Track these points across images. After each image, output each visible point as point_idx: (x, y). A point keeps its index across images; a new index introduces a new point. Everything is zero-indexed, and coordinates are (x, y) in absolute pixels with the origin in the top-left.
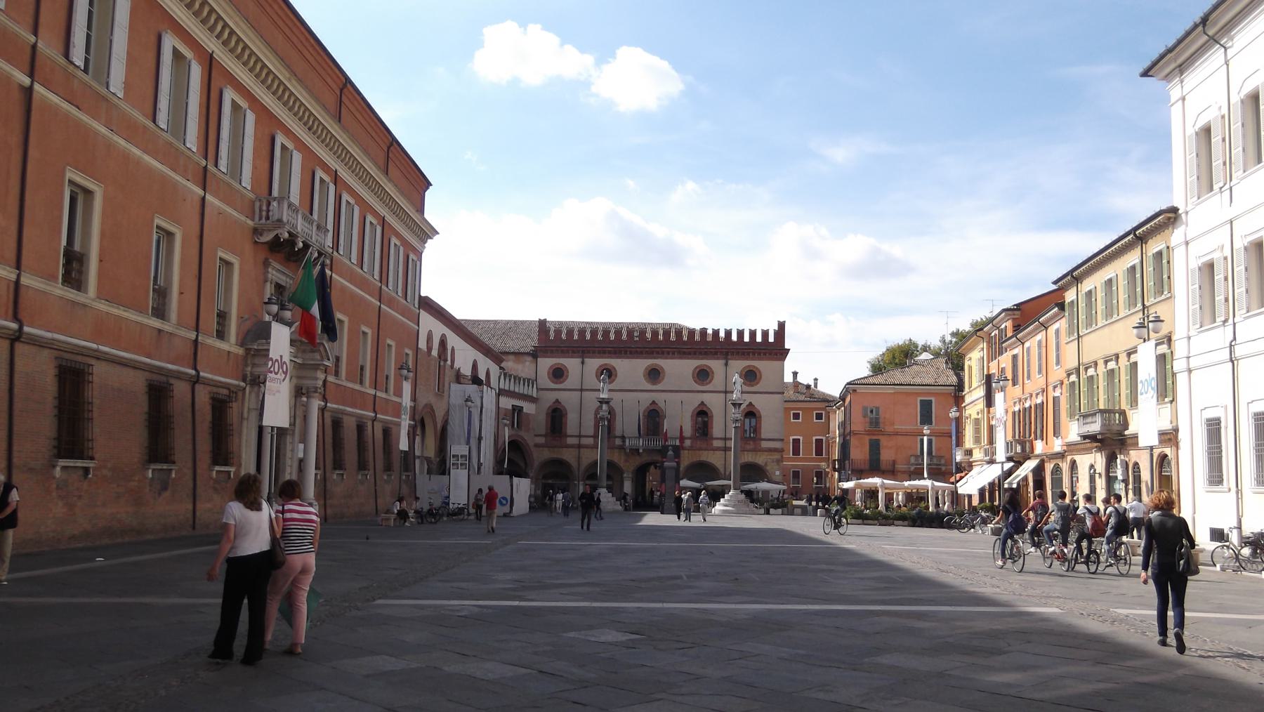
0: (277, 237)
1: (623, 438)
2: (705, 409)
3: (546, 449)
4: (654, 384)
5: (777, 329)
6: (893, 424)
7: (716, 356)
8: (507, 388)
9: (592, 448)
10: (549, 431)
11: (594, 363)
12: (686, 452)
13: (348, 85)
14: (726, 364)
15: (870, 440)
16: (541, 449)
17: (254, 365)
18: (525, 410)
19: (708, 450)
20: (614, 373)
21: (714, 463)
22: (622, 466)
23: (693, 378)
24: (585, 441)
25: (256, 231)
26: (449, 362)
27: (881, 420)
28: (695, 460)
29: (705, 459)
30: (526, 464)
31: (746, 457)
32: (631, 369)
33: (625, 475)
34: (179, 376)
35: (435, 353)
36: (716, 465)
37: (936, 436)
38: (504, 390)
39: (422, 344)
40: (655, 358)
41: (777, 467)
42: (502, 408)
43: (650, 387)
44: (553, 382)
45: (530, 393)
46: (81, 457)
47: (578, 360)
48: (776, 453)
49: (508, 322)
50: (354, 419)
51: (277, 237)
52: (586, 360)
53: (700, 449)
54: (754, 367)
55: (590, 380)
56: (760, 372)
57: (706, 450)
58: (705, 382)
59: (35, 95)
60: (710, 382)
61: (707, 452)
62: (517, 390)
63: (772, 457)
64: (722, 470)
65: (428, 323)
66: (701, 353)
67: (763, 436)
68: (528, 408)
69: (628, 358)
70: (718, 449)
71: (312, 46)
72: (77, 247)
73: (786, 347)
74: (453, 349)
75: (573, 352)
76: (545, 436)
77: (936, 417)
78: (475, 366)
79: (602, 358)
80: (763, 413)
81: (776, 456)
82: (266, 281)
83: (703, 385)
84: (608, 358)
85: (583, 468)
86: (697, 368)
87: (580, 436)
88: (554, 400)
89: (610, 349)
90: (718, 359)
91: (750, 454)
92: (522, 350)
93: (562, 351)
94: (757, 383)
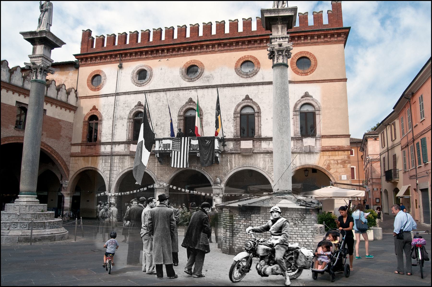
3: (82, 158)
5: (331, 9)
7: (262, 45)
10: (85, 140)
16: (77, 158)
40: (193, 54)
44: (92, 89)
48: (340, 152)
54: (308, 53)
56: (315, 58)
63: (336, 158)
69: (165, 57)
73: (345, 25)
79: (139, 59)
81: (341, 156)
86: (240, 59)
88: (91, 108)
94: (313, 71)
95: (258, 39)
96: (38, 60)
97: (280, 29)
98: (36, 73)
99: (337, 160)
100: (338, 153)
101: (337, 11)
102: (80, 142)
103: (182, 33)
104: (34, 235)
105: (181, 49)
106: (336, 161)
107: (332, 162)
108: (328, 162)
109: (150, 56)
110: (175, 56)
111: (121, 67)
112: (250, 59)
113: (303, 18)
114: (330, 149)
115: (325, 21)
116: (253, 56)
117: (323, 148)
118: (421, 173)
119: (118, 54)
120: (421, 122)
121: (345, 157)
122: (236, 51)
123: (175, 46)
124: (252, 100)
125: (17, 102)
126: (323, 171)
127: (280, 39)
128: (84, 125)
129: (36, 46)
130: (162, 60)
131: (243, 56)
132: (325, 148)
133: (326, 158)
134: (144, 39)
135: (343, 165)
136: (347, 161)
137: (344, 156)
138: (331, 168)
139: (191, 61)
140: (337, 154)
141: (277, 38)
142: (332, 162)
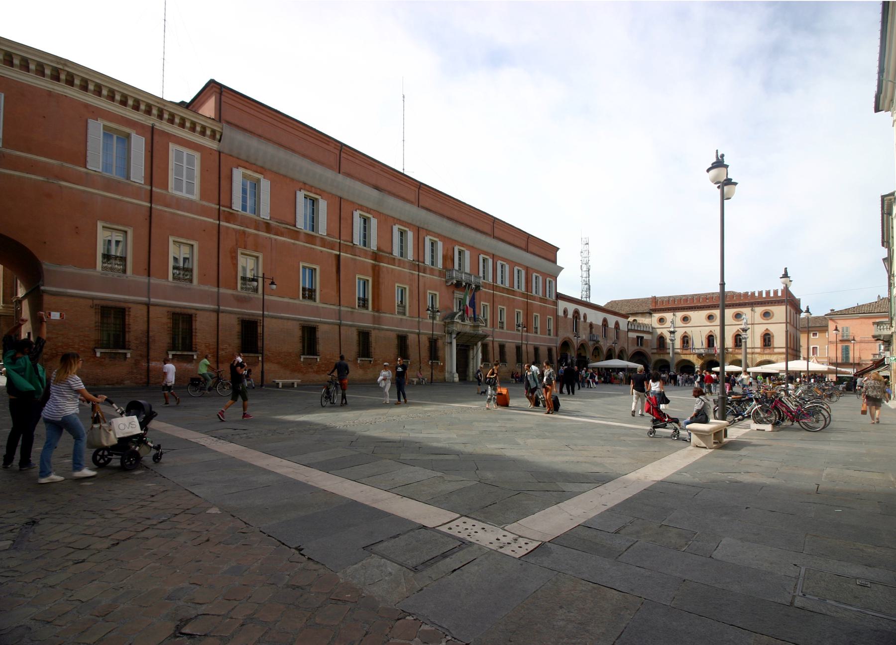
0: (452, 283)
4: (711, 322)
8: (633, 328)
11: (680, 314)
13: (496, 220)
15: (842, 346)
17: (448, 327)
18: (644, 338)
20: (689, 318)
25: (446, 282)
26: (582, 319)
30: (648, 362)
32: (698, 317)
33: (696, 367)
34: (412, 333)
35: (570, 316)
38: (631, 329)
39: (561, 313)
42: (630, 338)
43: (709, 324)
44: (660, 325)
45: (648, 330)
46: (368, 357)
49: (645, 299)
50: (514, 344)
51: (452, 283)
54: (769, 310)
55: (679, 322)
59: (341, 257)
62: (639, 329)
65: (562, 305)
67: (775, 346)
68: (646, 336)
69: (696, 311)
71: (473, 211)
72: (366, 297)
74: (585, 317)
76: (657, 349)
78: (605, 320)
80: (775, 334)
82: (454, 298)
83: (738, 321)
91: (767, 356)
92: (645, 312)
102: (655, 347)
115: (780, 294)
125: (637, 336)
128: (657, 341)
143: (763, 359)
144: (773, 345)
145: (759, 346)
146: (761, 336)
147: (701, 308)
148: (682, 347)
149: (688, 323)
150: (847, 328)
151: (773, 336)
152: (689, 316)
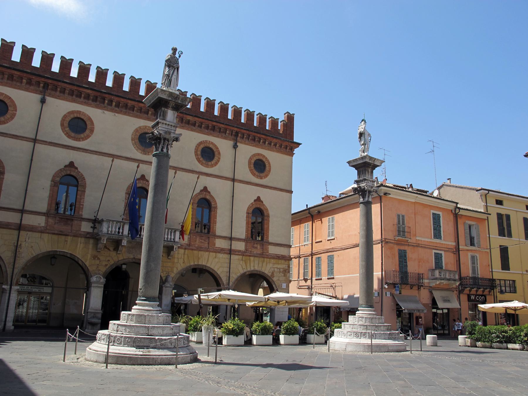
1: (96, 222)
2: (208, 197)
6: (415, 235)
9: (42, 232)
12: (182, 251)
14: (235, 147)
19: (210, 251)
20: (89, 126)
21: (216, 269)
22: (87, 264)
23: (196, 154)
24: (29, 220)
27: (406, 229)
28: (192, 264)
29: (204, 264)
31: (252, 265)
33: (94, 279)
36: (219, 272)
37: (445, 251)
41: (284, 278)
47: (36, 97)
48: (283, 261)
52: (49, 99)
53: (200, 249)
54: (264, 156)
57: (207, 250)
58: (210, 163)
60: (216, 163)
61: (207, 253)
63: (279, 266)
64: (224, 279)
66: (207, 128)
69: (112, 111)
70: (221, 251)
75: (29, 83)
77: (443, 232)
79: (73, 101)
80: (271, 213)
83: (207, 166)
84: (81, 103)
85: (21, 262)
86: (201, 143)
87: (22, 211)
89: (89, 91)
90: (225, 138)
93: (11, 78)
94: (266, 176)
95: (222, 127)
96: (171, 130)
97: (370, 173)
98: (167, 146)
99: (280, 269)
100: (281, 262)
101: (290, 124)
103: (136, 87)
104: (111, 353)
105: (135, 108)
106: (278, 269)
107: (276, 269)
108: (272, 269)
109: (90, 102)
110: (125, 114)
111: (43, 101)
112: (211, 146)
113: (263, 119)
114: (276, 257)
116: (214, 144)
117: (270, 255)
118: (317, 285)
119: (42, 82)
120: (328, 240)
121: (286, 266)
122: (197, 132)
123: (130, 102)
124: (209, 192)
126: (268, 278)
127: (370, 182)
129: (166, 109)
130: (106, 112)
131: (204, 140)
132: (271, 255)
133: (271, 265)
134: (83, 75)
135: (284, 274)
136: (287, 270)
137: (285, 265)
138: (274, 275)
139: (146, 126)
140: (280, 263)
141: (369, 180)
142: (276, 269)
143: (249, 269)
144: (268, 237)
145: (243, 236)
146: (248, 213)
147: (126, 106)
148: (53, 211)
149: (84, 139)
150: (403, 216)
151: (269, 217)
152: (90, 119)
